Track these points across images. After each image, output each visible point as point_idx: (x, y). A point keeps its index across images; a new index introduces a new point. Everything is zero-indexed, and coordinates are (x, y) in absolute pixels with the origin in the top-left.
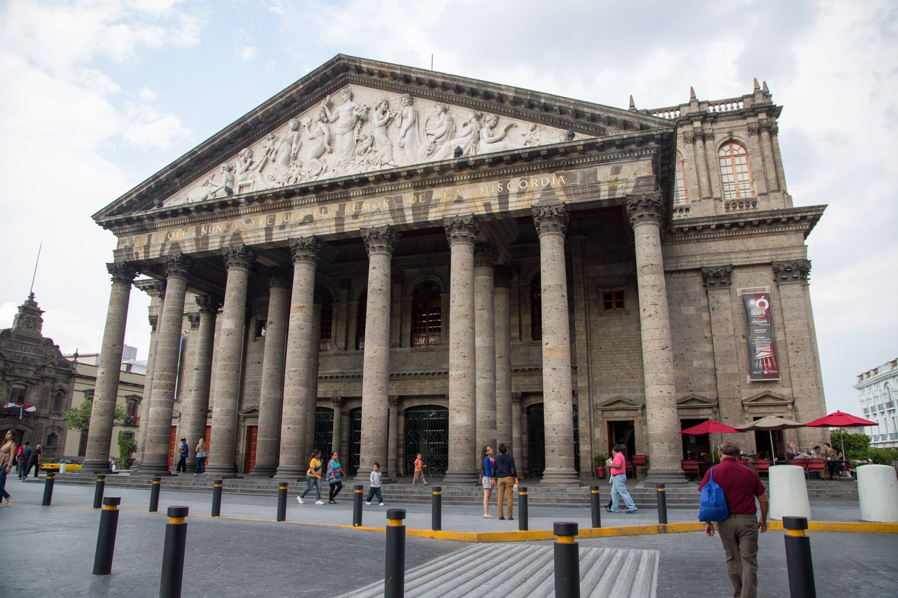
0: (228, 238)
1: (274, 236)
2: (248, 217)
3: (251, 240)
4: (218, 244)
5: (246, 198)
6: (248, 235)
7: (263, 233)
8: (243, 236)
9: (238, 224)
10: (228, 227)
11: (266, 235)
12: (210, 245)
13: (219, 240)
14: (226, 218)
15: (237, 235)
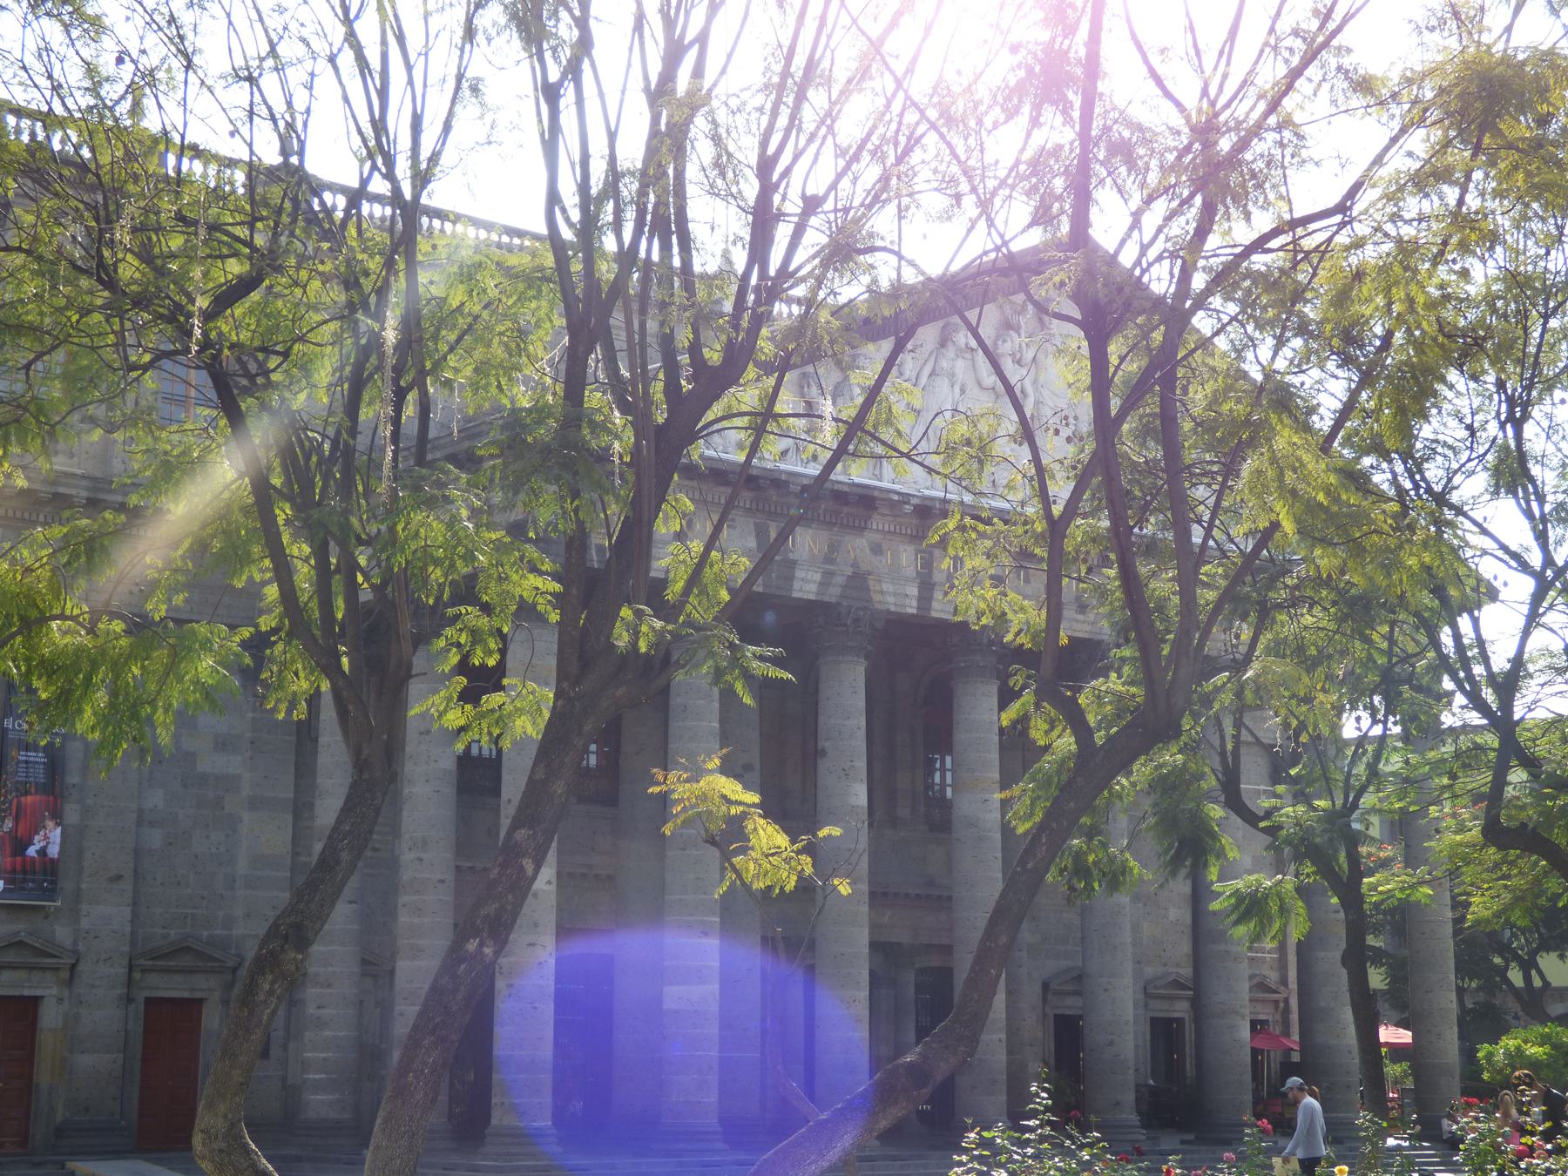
0: (840, 580)
1: (935, 605)
2: (878, 537)
3: (891, 599)
4: (813, 587)
5: (916, 507)
6: (885, 587)
7: (913, 591)
8: (871, 583)
9: (857, 547)
10: (833, 548)
11: (920, 599)
12: (796, 585)
13: (818, 577)
14: (829, 525)
15: (859, 580)
